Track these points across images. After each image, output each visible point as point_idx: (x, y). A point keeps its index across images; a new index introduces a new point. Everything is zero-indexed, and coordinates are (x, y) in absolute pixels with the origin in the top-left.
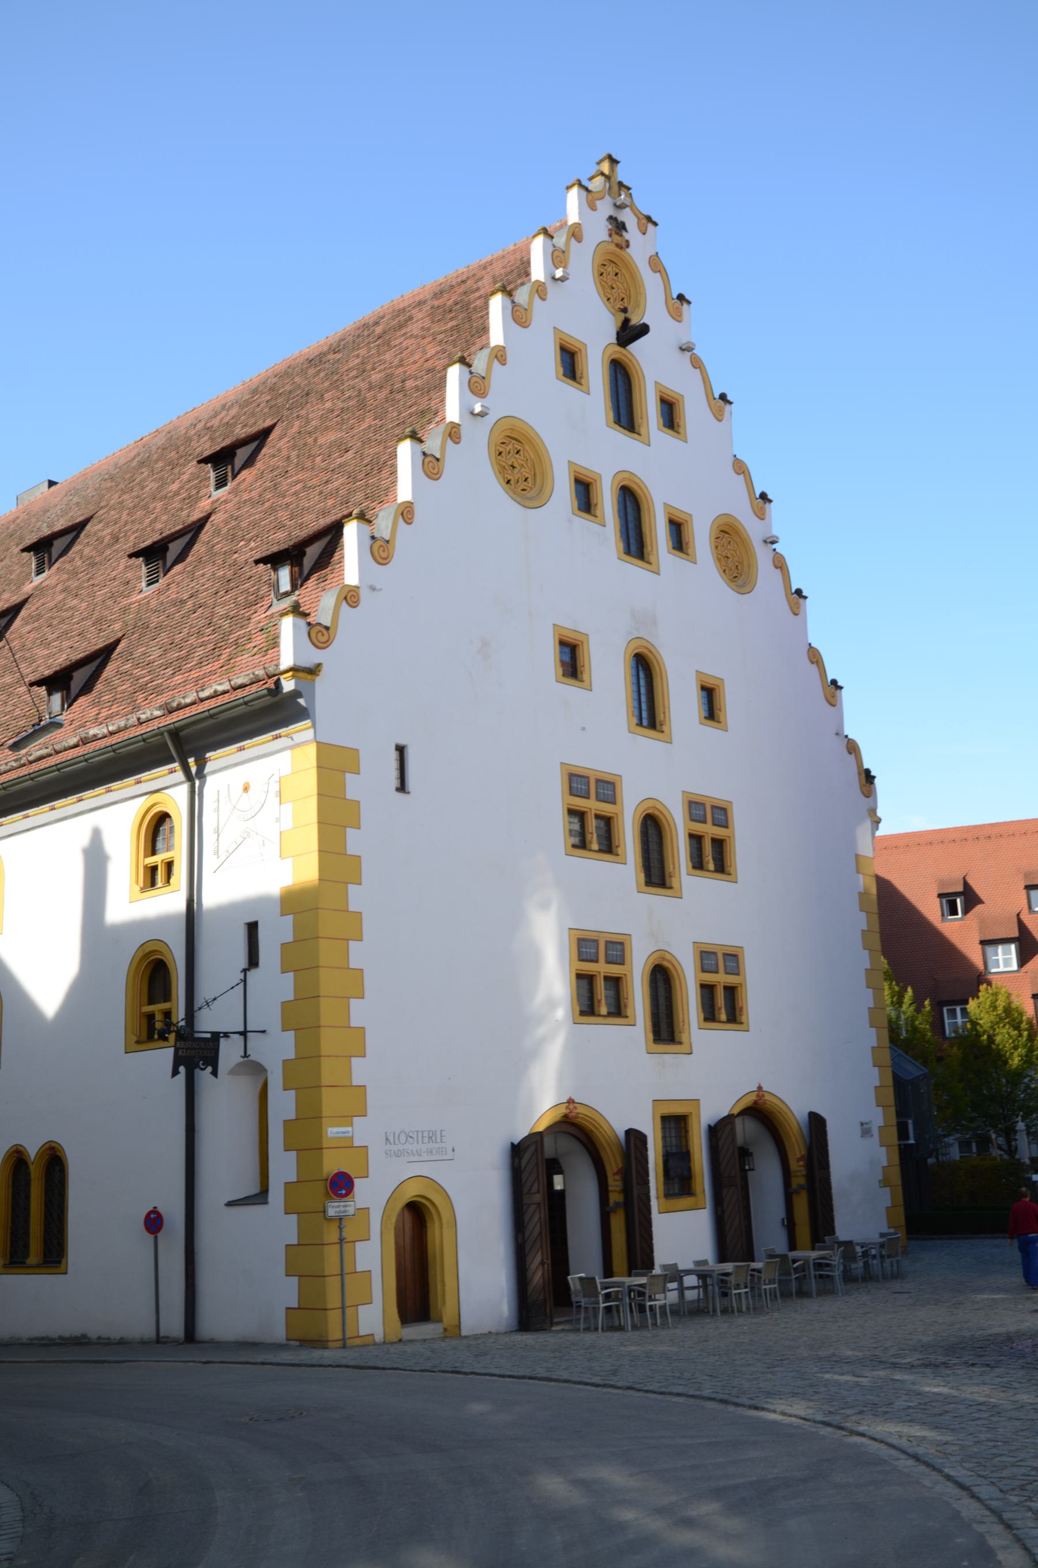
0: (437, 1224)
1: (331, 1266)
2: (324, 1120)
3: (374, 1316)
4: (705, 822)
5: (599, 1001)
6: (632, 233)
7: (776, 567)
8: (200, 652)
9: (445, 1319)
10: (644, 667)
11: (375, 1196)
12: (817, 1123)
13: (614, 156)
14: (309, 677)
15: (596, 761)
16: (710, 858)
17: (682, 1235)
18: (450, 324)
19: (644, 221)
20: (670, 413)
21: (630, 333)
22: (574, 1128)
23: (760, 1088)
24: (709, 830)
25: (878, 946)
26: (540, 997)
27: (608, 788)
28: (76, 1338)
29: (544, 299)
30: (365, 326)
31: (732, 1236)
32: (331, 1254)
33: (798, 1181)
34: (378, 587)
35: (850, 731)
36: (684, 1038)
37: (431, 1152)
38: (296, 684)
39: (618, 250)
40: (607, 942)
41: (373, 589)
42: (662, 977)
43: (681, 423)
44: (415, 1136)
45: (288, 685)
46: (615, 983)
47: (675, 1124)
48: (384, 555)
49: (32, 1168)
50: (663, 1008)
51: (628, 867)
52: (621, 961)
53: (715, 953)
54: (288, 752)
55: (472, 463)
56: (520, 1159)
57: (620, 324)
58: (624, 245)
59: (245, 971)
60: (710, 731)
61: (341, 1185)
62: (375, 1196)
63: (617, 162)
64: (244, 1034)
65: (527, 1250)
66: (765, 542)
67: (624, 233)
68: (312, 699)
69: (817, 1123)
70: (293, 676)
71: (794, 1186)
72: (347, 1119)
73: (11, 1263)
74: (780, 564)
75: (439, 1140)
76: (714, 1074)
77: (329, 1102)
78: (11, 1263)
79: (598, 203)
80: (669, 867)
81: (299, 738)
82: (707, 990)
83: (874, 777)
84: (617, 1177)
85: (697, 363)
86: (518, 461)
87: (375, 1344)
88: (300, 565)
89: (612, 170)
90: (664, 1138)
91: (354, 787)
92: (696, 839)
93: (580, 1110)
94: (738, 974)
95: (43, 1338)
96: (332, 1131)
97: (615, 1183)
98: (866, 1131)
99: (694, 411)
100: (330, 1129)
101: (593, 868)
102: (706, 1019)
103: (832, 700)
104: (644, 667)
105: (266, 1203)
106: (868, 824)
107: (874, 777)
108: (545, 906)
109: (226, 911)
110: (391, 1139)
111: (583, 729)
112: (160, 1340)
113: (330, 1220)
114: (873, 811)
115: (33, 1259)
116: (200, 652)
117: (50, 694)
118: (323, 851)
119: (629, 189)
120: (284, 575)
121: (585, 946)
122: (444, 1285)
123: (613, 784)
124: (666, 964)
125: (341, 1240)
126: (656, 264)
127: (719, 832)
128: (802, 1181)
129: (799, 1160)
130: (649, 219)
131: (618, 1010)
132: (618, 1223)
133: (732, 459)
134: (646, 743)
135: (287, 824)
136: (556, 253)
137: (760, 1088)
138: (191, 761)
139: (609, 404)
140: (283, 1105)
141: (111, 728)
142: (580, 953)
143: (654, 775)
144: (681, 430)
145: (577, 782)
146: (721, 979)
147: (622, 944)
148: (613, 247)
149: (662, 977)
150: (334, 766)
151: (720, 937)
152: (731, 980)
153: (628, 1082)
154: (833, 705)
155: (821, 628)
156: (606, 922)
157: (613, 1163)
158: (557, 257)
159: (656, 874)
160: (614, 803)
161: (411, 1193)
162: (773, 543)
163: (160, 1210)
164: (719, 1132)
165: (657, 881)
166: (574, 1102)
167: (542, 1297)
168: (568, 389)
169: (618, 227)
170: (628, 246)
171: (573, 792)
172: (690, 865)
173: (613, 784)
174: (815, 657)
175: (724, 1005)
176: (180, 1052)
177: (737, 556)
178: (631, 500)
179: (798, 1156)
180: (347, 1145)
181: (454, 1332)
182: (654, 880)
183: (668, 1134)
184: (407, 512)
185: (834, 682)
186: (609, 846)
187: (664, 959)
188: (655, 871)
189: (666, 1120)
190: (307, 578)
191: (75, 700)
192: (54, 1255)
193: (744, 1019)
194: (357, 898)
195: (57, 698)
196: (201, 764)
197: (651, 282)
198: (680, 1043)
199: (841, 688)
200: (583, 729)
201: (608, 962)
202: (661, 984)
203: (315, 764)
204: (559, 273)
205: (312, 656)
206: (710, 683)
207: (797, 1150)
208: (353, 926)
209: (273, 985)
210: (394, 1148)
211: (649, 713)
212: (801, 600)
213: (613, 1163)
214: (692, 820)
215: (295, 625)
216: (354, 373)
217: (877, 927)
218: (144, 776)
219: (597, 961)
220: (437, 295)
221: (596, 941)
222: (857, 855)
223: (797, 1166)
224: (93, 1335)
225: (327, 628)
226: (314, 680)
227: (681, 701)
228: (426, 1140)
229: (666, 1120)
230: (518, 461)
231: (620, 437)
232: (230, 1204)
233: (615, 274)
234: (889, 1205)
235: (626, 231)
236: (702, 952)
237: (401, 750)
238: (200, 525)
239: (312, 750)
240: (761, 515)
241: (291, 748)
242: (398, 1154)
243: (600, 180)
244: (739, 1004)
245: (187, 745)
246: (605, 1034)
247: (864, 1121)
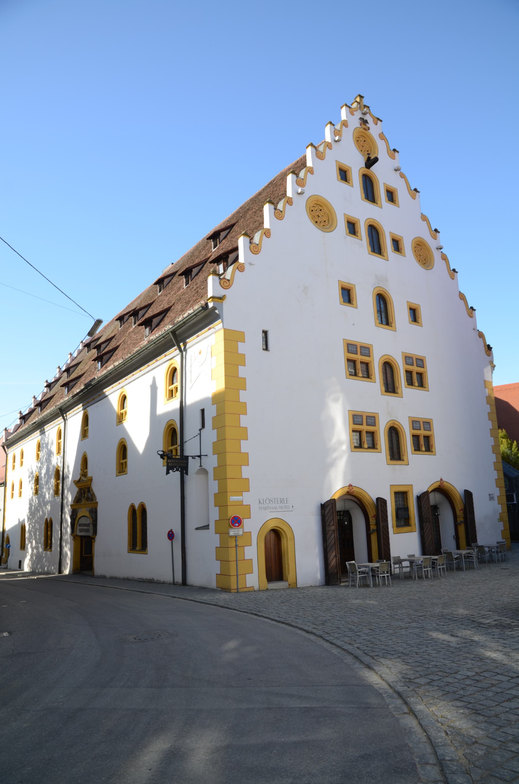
0: (285, 539)
1: (232, 557)
2: (228, 493)
3: (254, 578)
4: (413, 365)
5: (364, 442)
7: (443, 259)
9: (289, 580)
11: (254, 526)
12: (468, 494)
13: (362, 95)
14: (220, 301)
15: (360, 338)
16: (416, 381)
17: (405, 544)
19: (376, 120)
20: (391, 196)
21: (371, 162)
22: (353, 497)
23: (441, 480)
24: (415, 369)
25: (495, 419)
26: (334, 440)
27: (366, 350)
28: (150, 580)
29: (331, 149)
31: (430, 544)
32: (232, 551)
33: (460, 519)
34: (253, 263)
35: (480, 328)
36: (405, 458)
37: (282, 507)
38: (214, 304)
39: (364, 131)
40: (367, 417)
41: (251, 264)
43: (396, 200)
44: (273, 500)
45: (211, 305)
46: (372, 434)
47: (401, 496)
48: (256, 250)
49: (137, 512)
50: (395, 446)
51: (376, 384)
53: (419, 422)
54: (214, 335)
55: (297, 214)
56: (325, 511)
57: (366, 159)
58: (367, 129)
59: (200, 430)
60: (414, 327)
61: (237, 521)
62: (254, 526)
63: (363, 97)
64: (200, 456)
65: (328, 550)
66: (437, 249)
67: (367, 124)
68: (221, 310)
69: (468, 494)
70: (212, 300)
71: (459, 522)
72: (240, 493)
73: (133, 549)
74: (444, 258)
75: (285, 502)
76: (419, 474)
77: (231, 485)
78: (133, 549)
79: (355, 113)
80: (397, 384)
81: (217, 328)
82: (416, 438)
83: (492, 348)
84: (373, 519)
85: (402, 176)
86: (320, 214)
87: (255, 591)
88: (227, 261)
89: (361, 100)
90: (396, 501)
91: (242, 348)
93: (355, 489)
94: (430, 431)
95: (141, 579)
96: (233, 498)
97: (372, 521)
98: (491, 498)
99: (402, 195)
100: (231, 497)
101: (360, 385)
102: (415, 450)
103: (471, 315)
105: (209, 529)
106: (489, 367)
107: (492, 348)
108: (336, 400)
109: (193, 405)
110: (262, 502)
111: (354, 324)
112: (174, 583)
113: (231, 537)
114: (491, 362)
115: (138, 548)
117: (146, 328)
118: (227, 376)
119: (369, 107)
121: (356, 418)
122: (288, 565)
123: (369, 348)
124: (396, 426)
125: (236, 546)
126: (382, 136)
127: (420, 370)
128: (462, 519)
129: (460, 511)
130: (378, 119)
131: (373, 446)
132: (374, 538)
133: (420, 215)
134: (384, 331)
136: (336, 131)
137: (441, 480)
138: (181, 344)
139: (363, 191)
141: (157, 335)
142: (354, 421)
144: (396, 202)
145: (351, 347)
146: (422, 433)
147: (374, 417)
148: (362, 130)
149: (394, 432)
150: (232, 340)
151: (421, 414)
152: (427, 433)
153: (379, 478)
154: (472, 317)
155: (464, 284)
157: (372, 513)
158: (336, 132)
159: (390, 387)
160: (369, 356)
161: (272, 525)
162: (441, 249)
163: (173, 531)
164: (422, 498)
165: (391, 390)
166: (352, 486)
167: (335, 571)
168: (343, 185)
169: (364, 122)
170: (369, 129)
172: (406, 383)
173: (369, 348)
174: (462, 297)
175: (424, 444)
176: (170, 464)
179: (460, 509)
180: (240, 504)
181: (294, 586)
182: (389, 390)
183: (398, 500)
185: (472, 308)
186: (368, 375)
187: (395, 424)
188: (390, 386)
189: (396, 493)
191: (154, 330)
192: (144, 547)
193: (433, 450)
194: (244, 396)
195: (148, 329)
196: (185, 345)
197: (381, 145)
198: (403, 460)
199: (475, 310)
200: (354, 324)
201: (367, 425)
202: (394, 435)
203: (223, 338)
204: (337, 138)
205: (221, 292)
206: (413, 307)
207: (459, 506)
208: (243, 409)
209: (210, 435)
210: (263, 505)
212: (455, 273)
213: (372, 513)
214: (407, 364)
215: (213, 279)
217: (495, 411)
218: (167, 353)
219: (362, 425)
221: (362, 416)
222: (485, 381)
223: (459, 513)
224: (156, 579)
225: (228, 280)
226: (222, 302)
227: (400, 313)
228: (279, 502)
229: (396, 493)
230: (320, 214)
231: (368, 205)
232: (197, 529)
233: (363, 140)
234: (503, 529)
235: (368, 123)
236: (413, 421)
237: (265, 333)
240: (435, 238)
241: (215, 332)
242: (265, 509)
243: (356, 104)
244: (431, 443)
245: (179, 338)
246: (367, 456)
247: (490, 493)
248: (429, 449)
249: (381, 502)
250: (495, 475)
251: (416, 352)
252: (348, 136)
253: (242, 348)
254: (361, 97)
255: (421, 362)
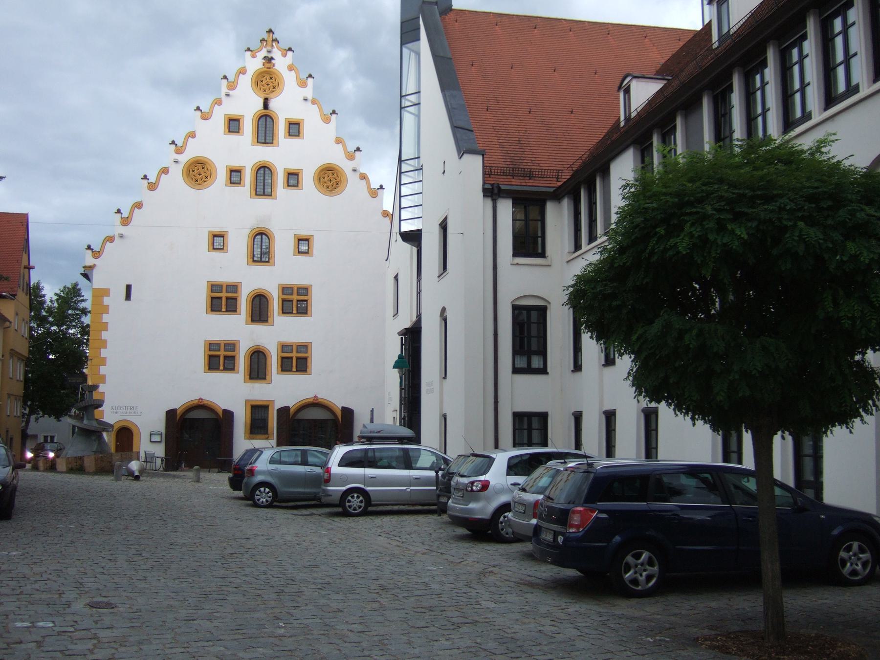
4: (292, 294)
20: (295, 128)
23: (316, 397)
27: (234, 288)
74: (363, 177)
91: (106, 301)
137: (316, 397)
143: (253, 280)
164: (283, 411)
169: (269, 60)
178: (264, 170)
237: (129, 288)
249: (229, 415)
252: (245, 82)
253: (106, 301)
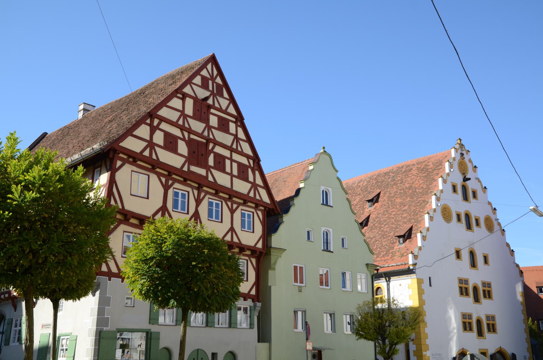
6: (465, 156)
8: (382, 254)
10: (472, 254)
15: (464, 276)
18: (424, 175)
21: (466, 179)
24: (487, 289)
25: (526, 313)
27: (466, 282)
30: (399, 168)
35: (517, 262)
42: (479, 322)
46: (470, 323)
51: (471, 299)
52: (471, 319)
55: (439, 216)
60: (486, 266)
69: (514, 356)
72: (426, 351)
74: (499, 224)
76: (491, 343)
80: (479, 298)
82: (488, 325)
85: (479, 181)
86: (446, 213)
92: (484, 291)
96: (424, 353)
99: (479, 193)
101: (464, 299)
104: (472, 254)
116: (382, 254)
118: (419, 299)
120: (401, 240)
121: (464, 316)
126: (470, 161)
131: (471, 329)
134: (473, 271)
135: (411, 293)
140: (412, 347)
143: (475, 278)
145: (461, 281)
146: (491, 322)
149: (479, 322)
150: (420, 282)
151: (490, 313)
152: (493, 322)
155: (509, 238)
156: (468, 311)
158: (451, 166)
159: (477, 300)
169: (462, 154)
171: (460, 283)
174: (508, 245)
175: (492, 328)
177: (490, 224)
184: (428, 229)
185: (512, 250)
186: (467, 294)
190: (406, 241)
205: (416, 261)
206: (485, 255)
211: (473, 264)
216: (400, 182)
217: (525, 309)
220: (418, 163)
227: (480, 260)
230: (446, 213)
231: (465, 203)
233: (463, 168)
237: (430, 278)
238: (368, 218)
239: (416, 280)
240: (495, 213)
243: (458, 145)
246: (468, 334)
248: (494, 330)
250: (526, 345)
251: (487, 280)
254: (460, 140)
255: (489, 285)
